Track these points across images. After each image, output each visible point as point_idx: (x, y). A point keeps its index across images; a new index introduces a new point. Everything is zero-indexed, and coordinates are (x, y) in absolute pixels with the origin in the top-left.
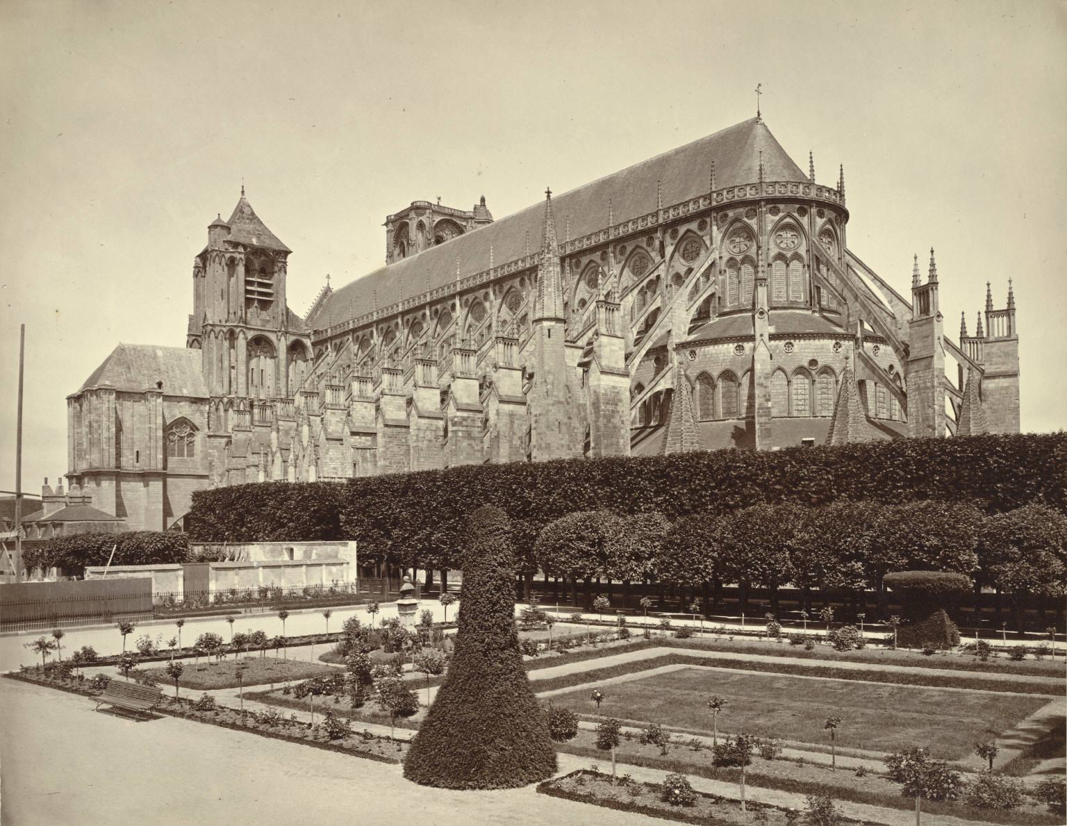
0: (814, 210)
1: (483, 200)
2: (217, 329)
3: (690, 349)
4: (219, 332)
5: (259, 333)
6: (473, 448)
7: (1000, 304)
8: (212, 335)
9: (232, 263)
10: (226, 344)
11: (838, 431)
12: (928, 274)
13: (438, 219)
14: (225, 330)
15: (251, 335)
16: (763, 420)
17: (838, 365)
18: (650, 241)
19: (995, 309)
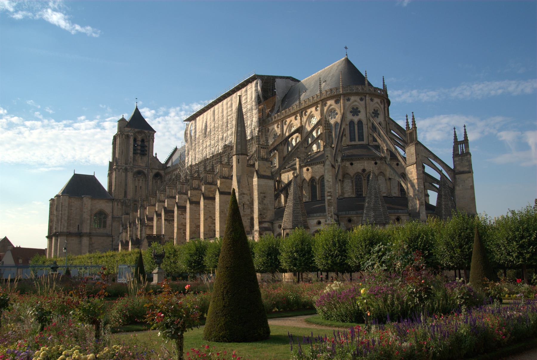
0: (368, 98)
2: (120, 167)
3: (306, 168)
4: (120, 169)
5: (140, 169)
6: (212, 218)
7: (461, 138)
8: (117, 170)
9: (128, 137)
10: (123, 174)
11: (368, 202)
12: (412, 123)
14: (123, 168)
15: (135, 170)
16: (329, 198)
17: (377, 171)
18: (296, 119)
19: (458, 140)
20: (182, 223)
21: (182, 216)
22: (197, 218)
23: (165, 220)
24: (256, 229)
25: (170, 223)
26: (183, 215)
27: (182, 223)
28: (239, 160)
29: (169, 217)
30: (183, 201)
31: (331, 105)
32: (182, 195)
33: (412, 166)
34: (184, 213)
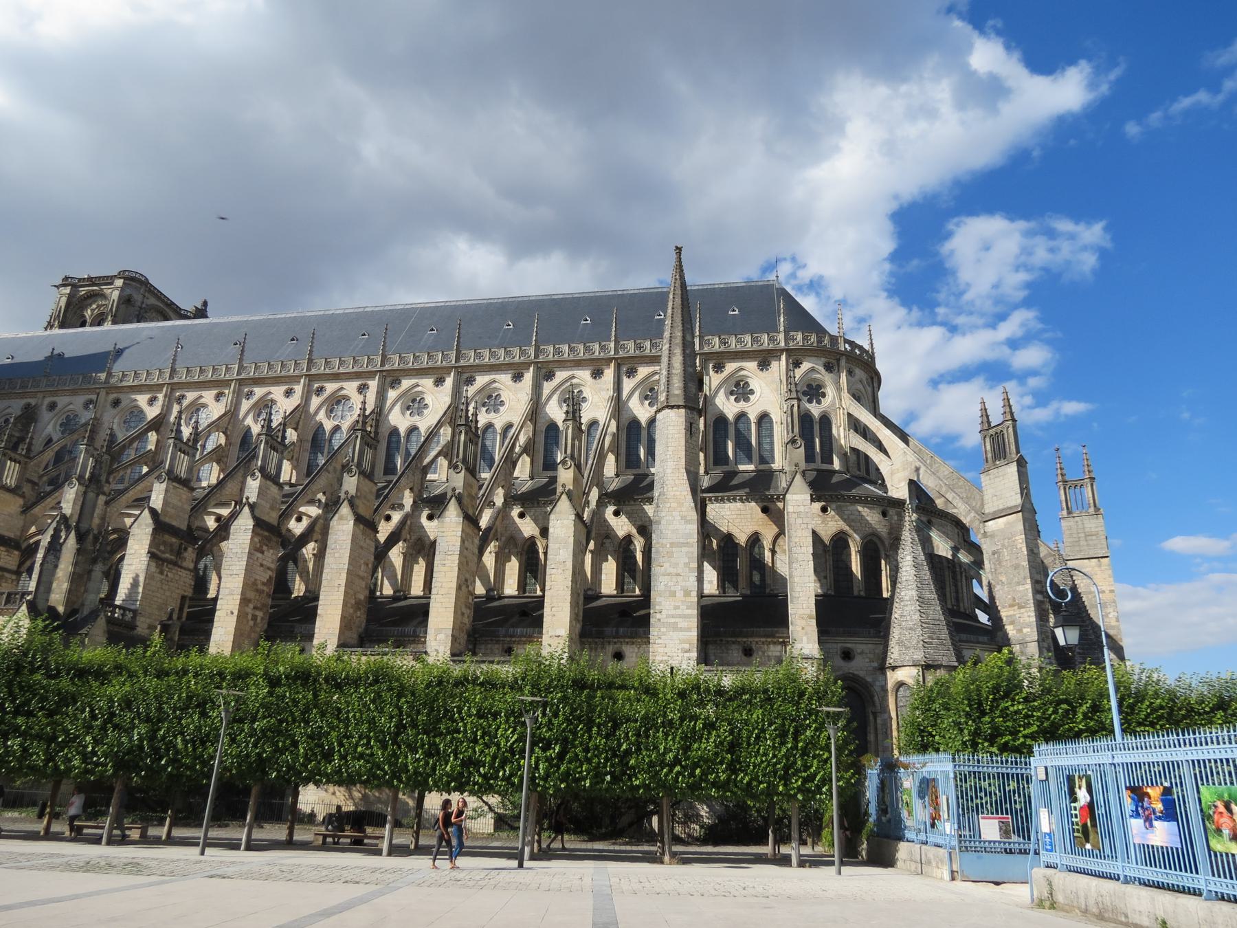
1: (205, 304)
6: (468, 587)
13: (152, 301)
20: (256, 580)
21: (259, 555)
22: (361, 574)
23: (153, 555)
24: (806, 652)
25: (161, 573)
26: (262, 552)
27: (255, 583)
28: (691, 424)
29: (162, 548)
30: (268, 506)
31: (813, 370)
32: (268, 482)
33: (1096, 560)
34: (265, 548)
